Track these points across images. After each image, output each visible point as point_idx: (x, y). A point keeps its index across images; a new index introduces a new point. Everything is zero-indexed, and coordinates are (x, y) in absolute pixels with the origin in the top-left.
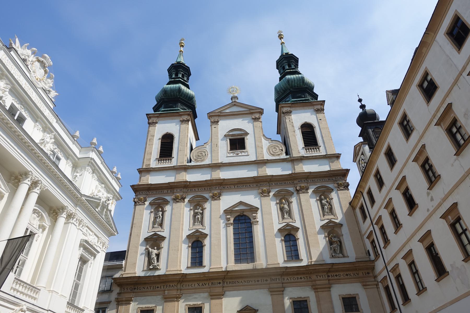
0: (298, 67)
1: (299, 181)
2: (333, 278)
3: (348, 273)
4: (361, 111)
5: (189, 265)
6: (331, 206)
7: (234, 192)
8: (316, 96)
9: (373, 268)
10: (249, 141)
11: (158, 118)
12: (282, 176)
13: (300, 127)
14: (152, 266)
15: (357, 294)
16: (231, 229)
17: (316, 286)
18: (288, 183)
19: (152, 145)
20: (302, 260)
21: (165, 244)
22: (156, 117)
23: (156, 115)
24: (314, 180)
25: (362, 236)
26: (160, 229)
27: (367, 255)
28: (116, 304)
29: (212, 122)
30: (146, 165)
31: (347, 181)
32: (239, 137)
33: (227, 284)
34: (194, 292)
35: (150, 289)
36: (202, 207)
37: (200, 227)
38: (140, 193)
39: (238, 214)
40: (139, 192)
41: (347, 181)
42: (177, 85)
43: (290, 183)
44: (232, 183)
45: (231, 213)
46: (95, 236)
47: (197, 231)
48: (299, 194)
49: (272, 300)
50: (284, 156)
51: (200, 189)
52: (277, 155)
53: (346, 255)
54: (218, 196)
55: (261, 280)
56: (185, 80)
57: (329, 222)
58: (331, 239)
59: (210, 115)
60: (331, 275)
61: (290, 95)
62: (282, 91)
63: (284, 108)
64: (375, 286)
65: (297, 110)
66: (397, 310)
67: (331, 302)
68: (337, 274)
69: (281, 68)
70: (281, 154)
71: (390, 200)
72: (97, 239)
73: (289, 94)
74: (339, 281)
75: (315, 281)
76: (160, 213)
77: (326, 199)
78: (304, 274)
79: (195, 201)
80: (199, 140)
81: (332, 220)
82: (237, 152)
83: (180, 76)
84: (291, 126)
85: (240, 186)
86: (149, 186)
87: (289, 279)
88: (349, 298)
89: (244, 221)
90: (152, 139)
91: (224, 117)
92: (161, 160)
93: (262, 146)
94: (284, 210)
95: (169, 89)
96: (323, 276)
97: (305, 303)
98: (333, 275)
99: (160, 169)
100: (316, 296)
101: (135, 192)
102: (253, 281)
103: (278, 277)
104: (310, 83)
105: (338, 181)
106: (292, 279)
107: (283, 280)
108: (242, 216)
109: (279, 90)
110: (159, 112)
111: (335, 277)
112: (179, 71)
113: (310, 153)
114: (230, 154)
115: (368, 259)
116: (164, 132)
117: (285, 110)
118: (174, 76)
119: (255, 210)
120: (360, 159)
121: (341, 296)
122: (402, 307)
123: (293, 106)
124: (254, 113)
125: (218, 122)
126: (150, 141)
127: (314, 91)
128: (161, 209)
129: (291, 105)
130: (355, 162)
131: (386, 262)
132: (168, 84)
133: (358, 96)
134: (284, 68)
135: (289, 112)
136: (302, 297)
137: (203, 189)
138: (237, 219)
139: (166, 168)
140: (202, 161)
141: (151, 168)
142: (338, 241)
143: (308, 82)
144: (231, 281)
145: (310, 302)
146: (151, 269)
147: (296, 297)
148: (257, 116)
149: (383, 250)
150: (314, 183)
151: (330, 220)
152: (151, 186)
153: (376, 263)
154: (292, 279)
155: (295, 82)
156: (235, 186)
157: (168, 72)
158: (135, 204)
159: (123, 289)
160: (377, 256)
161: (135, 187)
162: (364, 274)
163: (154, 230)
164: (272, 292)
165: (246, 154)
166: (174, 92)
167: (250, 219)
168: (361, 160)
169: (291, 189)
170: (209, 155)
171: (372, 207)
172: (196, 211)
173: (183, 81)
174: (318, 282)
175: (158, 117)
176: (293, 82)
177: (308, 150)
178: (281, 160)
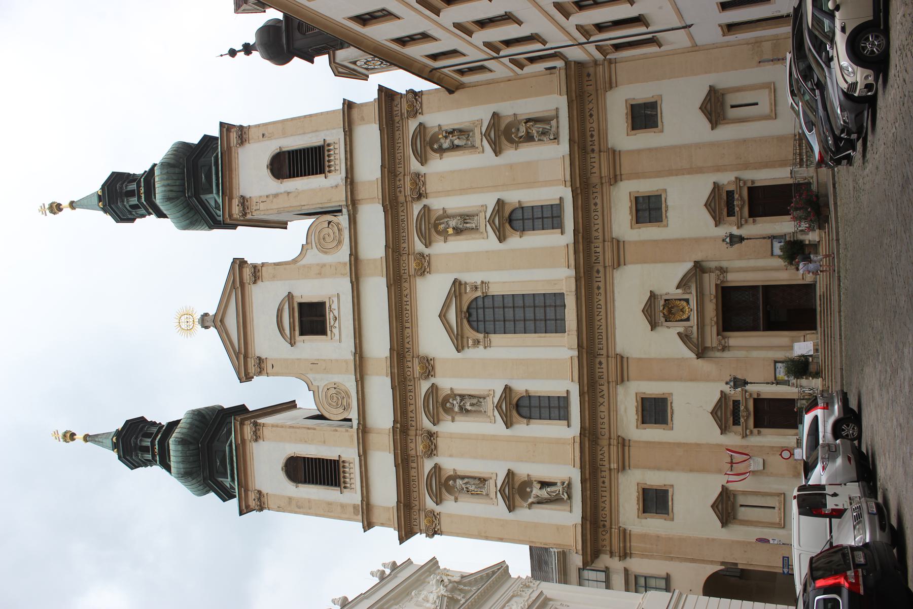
0: (134, 174)
1: (400, 192)
2: (596, 143)
4: (256, 54)
5: (565, 422)
6: (454, 130)
7: (419, 329)
8: (207, 141)
9: (580, 65)
10: (308, 292)
11: (248, 490)
12: (389, 227)
13: (280, 181)
14: (563, 494)
15: (626, 101)
16: (496, 339)
17: (611, 177)
18: (402, 214)
19: (309, 501)
21: (523, 470)
22: (247, 494)
25: (517, 78)
26: (492, 482)
27: (555, 74)
28: (630, 558)
29: (260, 372)
30: (356, 513)
31: (404, 92)
32: (296, 314)
33: (602, 349)
34: (615, 413)
35: (606, 496)
37: (489, 400)
38: (415, 523)
39: (465, 322)
40: (414, 526)
41: (404, 92)
42: (172, 447)
43: (402, 211)
46: (513, 602)
47: (498, 407)
48: (428, 195)
50: (343, 220)
52: (340, 234)
53: (554, 113)
54: (427, 365)
55: (597, 282)
56: (156, 430)
57: (489, 138)
58: (521, 137)
59: (245, 376)
60: (591, 145)
61: (201, 196)
62: (190, 215)
63: (234, 212)
64: (613, 66)
65: (239, 184)
66: (655, 36)
67: (639, 151)
68: (589, 134)
69: (134, 213)
70: (338, 224)
71: (457, 26)
72: (515, 599)
74: (602, 134)
75: (601, 178)
76: (459, 482)
80: (295, 401)
81: (483, 134)
82: (329, 319)
83: (147, 443)
85: (407, 315)
86: (402, 507)
87: (597, 227)
88: (632, 118)
89: (481, 311)
91: (250, 347)
92: (345, 482)
93: (318, 265)
94: (461, 226)
95: (181, 466)
96: (593, 162)
97: (641, 199)
98: (591, 141)
100: (629, 179)
101: (415, 534)
102: (598, 297)
103: (593, 249)
104: (175, 151)
105: (403, 111)
106: (596, 222)
107: (599, 239)
108: (470, 315)
109: (187, 221)
110: (235, 489)
111: (595, 138)
112: (136, 444)
113: (339, 163)
115: (563, 73)
116: (282, 476)
117: (236, 210)
118: (149, 457)
119: (457, 287)
120: (363, 66)
121: (629, 132)
122: (650, 29)
123: (228, 191)
124: (242, 279)
125: (260, 358)
127: (197, 143)
128: (451, 482)
129: (226, 196)
130: (368, 77)
131: (570, 43)
132: (168, 469)
133: (221, 56)
134: (135, 207)
135: (244, 202)
136: (630, 205)
137: (410, 394)
138: (475, 324)
140: (348, 396)
141: (362, 503)
142: (526, 125)
143: (172, 156)
145: (638, 192)
146: (570, 497)
147: (630, 217)
148: (247, 272)
149: (548, 46)
150: (405, 162)
152: (403, 501)
153: (570, 59)
154: (596, 222)
156: (406, 328)
157: (136, 467)
158: (439, 534)
159: (604, 548)
161: (404, 536)
162: (590, 83)
163: (493, 495)
164: (619, 263)
165: (336, 300)
166: (188, 455)
168: (366, 66)
169: (417, 208)
171: (464, 55)
172: (456, 409)
173: (160, 436)
174: (604, 172)
175: (246, 490)
177: (332, 168)
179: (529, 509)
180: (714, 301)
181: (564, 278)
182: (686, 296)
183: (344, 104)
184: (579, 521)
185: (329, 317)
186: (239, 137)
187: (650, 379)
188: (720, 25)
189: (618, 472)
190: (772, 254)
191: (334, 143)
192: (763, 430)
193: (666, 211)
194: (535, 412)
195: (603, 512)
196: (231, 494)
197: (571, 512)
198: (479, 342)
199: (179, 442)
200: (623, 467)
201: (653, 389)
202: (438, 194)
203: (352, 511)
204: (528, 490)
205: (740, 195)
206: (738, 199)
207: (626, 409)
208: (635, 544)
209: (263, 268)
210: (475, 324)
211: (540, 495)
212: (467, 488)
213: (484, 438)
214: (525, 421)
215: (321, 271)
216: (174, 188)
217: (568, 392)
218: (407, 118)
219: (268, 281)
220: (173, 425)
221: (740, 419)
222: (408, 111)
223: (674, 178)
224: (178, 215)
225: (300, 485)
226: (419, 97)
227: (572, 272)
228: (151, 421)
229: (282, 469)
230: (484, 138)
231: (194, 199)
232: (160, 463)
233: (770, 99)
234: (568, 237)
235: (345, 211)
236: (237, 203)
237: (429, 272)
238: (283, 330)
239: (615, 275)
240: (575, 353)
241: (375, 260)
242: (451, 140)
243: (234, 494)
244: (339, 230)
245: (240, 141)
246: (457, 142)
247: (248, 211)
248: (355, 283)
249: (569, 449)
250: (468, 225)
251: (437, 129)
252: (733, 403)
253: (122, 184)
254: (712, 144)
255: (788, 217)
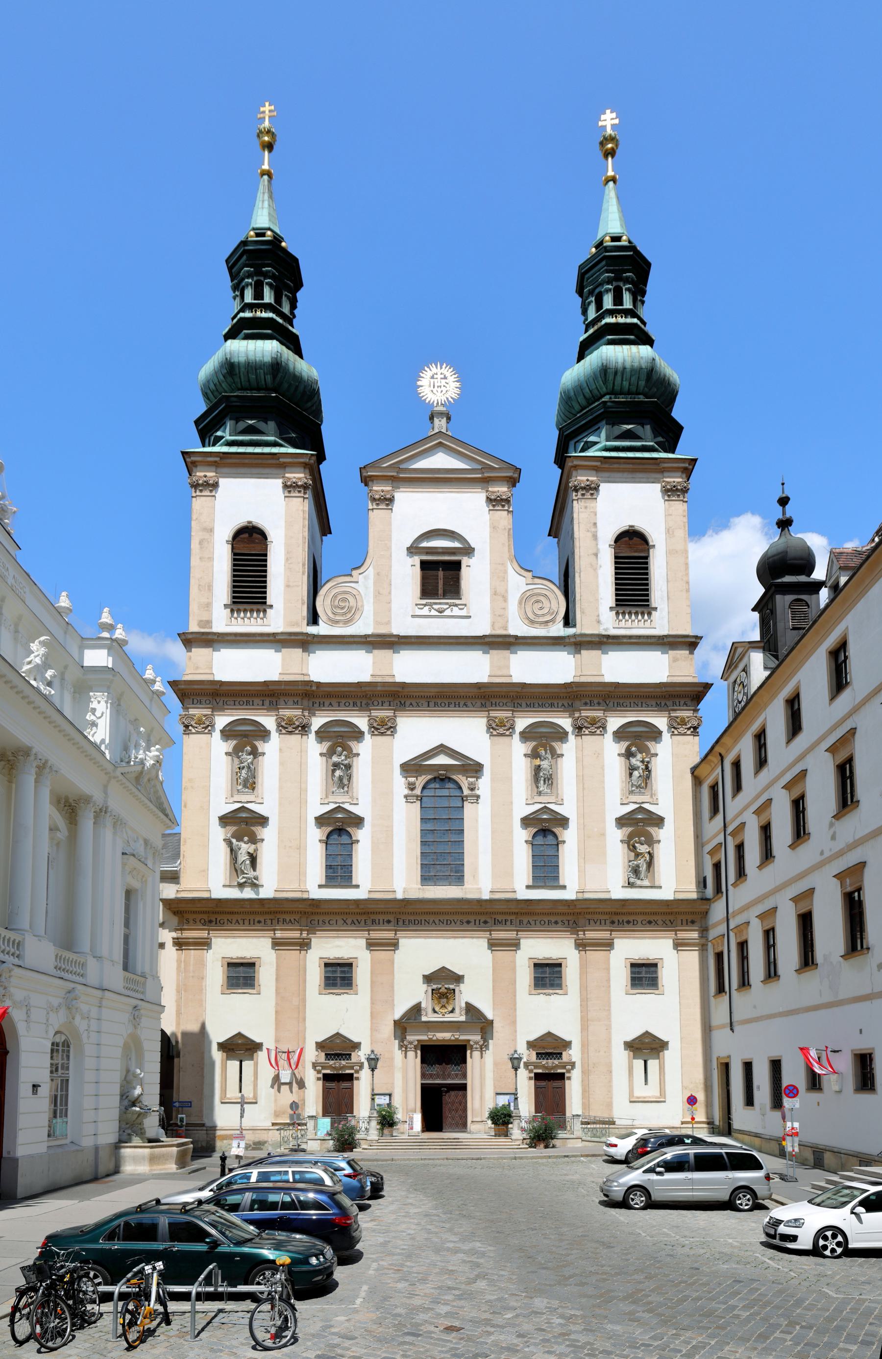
1: (586, 704)
3: (652, 920)
5: (323, 883)
6: (650, 771)
13: (613, 543)
14: (244, 878)
18: (560, 705)
19: (211, 559)
20: (564, 887)
21: (268, 834)
23: (211, 457)
24: (621, 702)
30: (201, 623)
36: (350, 750)
43: (563, 705)
44: (422, 694)
45: (417, 771)
47: (339, 809)
49: (493, 959)
50: (558, 629)
51: (343, 702)
52: (541, 623)
54: (386, 727)
61: (604, 422)
67: (608, 969)
70: (553, 621)
73: (602, 420)
77: (641, 753)
78: (563, 914)
79: (332, 734)
81: (643, 805)
84: (590, 535)
90: (208, 542)
92: (239, 611)
93: (506, 591)
94: (541, 774)
99: (238, 638)
102: (459, 922)
103: (509, 918)
110: (214, 445)
114: (422, 609)
118: (249, 298)
123: (606, 466)
126: (201, 548)
128: (249, 748)
135: (591, 489)
137: (352, 704)
139: (254, 638)
140: (348, 622)
144: (412, 918)
147: (541, 957)
151: (640, 807)
155: (625, 376)
160: (718, 890)
165: (463, 613)
167: (460, 788)
169: (565, 722)
170: (366, 608)
172: (335, 759)
173: (280, 321)
176: (619, 374)
177: (621, 617)
178: (549, 641)
179: (224, 840)
180: (453, 1038)
181: (479, 886)
182: (457, 1010)
183: (696, 637)
184: (214, 896)
185: (441, 603)
186: (674, 487)
187: (373, 973)
188: (729, 1057)
189: (273, 939)
190: (497, 1094)
191: (651, 621)
192: (321, 1083)
193: (545, 994)
194: (334, 850)
195: (226, 921)
196: (206, 435)
197: (224, 886)
198: (412, 789)
199: (276, 359)
200: (277, 944)
201: (362, 975)
202: (580, 749)
203: (204, 619)
204: (246, 839)
205: (557, 1067)
206: (553, 1063)
207: (338, 946)
208: (193, 954)
209: (506, 512)
210: (432, 786)
211: (240, 852)
212: (243, 768)
213: (303, 791)
214: (324, 838)
215: (499, 595)
216: (619, 378)
217: (357, 886)
218: (670, 717)
219: (490, 519)
220: (293, 343)
221: (332, 1060)
222: (677, 717)
223: (579, 1003)
224: (582, 378)
225: (230, 546)
226: (692, 732)
227: (486, 896)
228: (297, 301)
229: (250, 522)
230: (638, 806)
231: (602, 410)
232: (241, 318)
233: (650, 1097)
234: (524, 894)
235: (570, 631)
236: (590, 478)
237: (492, 735)
238: (427, 538)
239: (481, 940)
240: (400, 896)
241: (508, 667)
242: (639, 767)
243: (207, 441)
244: (547, 622)
245: (669, 487)
246: (636, 774)
247: (579, 494)
248: (483, 641)
249: (295, 886)
250: (542, 782)
251: (653, 751)
252: (348, 1054)
253: (632, 282)
254: (609, 1041)
255: (533, 1109)
